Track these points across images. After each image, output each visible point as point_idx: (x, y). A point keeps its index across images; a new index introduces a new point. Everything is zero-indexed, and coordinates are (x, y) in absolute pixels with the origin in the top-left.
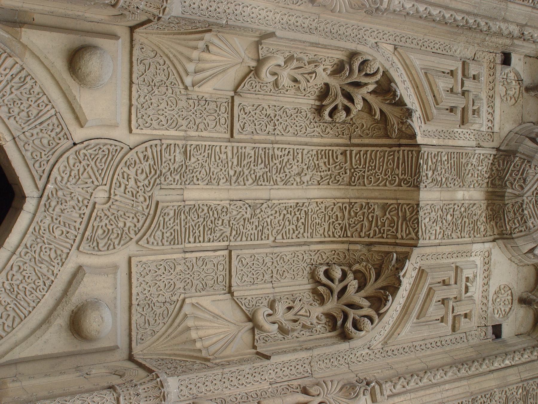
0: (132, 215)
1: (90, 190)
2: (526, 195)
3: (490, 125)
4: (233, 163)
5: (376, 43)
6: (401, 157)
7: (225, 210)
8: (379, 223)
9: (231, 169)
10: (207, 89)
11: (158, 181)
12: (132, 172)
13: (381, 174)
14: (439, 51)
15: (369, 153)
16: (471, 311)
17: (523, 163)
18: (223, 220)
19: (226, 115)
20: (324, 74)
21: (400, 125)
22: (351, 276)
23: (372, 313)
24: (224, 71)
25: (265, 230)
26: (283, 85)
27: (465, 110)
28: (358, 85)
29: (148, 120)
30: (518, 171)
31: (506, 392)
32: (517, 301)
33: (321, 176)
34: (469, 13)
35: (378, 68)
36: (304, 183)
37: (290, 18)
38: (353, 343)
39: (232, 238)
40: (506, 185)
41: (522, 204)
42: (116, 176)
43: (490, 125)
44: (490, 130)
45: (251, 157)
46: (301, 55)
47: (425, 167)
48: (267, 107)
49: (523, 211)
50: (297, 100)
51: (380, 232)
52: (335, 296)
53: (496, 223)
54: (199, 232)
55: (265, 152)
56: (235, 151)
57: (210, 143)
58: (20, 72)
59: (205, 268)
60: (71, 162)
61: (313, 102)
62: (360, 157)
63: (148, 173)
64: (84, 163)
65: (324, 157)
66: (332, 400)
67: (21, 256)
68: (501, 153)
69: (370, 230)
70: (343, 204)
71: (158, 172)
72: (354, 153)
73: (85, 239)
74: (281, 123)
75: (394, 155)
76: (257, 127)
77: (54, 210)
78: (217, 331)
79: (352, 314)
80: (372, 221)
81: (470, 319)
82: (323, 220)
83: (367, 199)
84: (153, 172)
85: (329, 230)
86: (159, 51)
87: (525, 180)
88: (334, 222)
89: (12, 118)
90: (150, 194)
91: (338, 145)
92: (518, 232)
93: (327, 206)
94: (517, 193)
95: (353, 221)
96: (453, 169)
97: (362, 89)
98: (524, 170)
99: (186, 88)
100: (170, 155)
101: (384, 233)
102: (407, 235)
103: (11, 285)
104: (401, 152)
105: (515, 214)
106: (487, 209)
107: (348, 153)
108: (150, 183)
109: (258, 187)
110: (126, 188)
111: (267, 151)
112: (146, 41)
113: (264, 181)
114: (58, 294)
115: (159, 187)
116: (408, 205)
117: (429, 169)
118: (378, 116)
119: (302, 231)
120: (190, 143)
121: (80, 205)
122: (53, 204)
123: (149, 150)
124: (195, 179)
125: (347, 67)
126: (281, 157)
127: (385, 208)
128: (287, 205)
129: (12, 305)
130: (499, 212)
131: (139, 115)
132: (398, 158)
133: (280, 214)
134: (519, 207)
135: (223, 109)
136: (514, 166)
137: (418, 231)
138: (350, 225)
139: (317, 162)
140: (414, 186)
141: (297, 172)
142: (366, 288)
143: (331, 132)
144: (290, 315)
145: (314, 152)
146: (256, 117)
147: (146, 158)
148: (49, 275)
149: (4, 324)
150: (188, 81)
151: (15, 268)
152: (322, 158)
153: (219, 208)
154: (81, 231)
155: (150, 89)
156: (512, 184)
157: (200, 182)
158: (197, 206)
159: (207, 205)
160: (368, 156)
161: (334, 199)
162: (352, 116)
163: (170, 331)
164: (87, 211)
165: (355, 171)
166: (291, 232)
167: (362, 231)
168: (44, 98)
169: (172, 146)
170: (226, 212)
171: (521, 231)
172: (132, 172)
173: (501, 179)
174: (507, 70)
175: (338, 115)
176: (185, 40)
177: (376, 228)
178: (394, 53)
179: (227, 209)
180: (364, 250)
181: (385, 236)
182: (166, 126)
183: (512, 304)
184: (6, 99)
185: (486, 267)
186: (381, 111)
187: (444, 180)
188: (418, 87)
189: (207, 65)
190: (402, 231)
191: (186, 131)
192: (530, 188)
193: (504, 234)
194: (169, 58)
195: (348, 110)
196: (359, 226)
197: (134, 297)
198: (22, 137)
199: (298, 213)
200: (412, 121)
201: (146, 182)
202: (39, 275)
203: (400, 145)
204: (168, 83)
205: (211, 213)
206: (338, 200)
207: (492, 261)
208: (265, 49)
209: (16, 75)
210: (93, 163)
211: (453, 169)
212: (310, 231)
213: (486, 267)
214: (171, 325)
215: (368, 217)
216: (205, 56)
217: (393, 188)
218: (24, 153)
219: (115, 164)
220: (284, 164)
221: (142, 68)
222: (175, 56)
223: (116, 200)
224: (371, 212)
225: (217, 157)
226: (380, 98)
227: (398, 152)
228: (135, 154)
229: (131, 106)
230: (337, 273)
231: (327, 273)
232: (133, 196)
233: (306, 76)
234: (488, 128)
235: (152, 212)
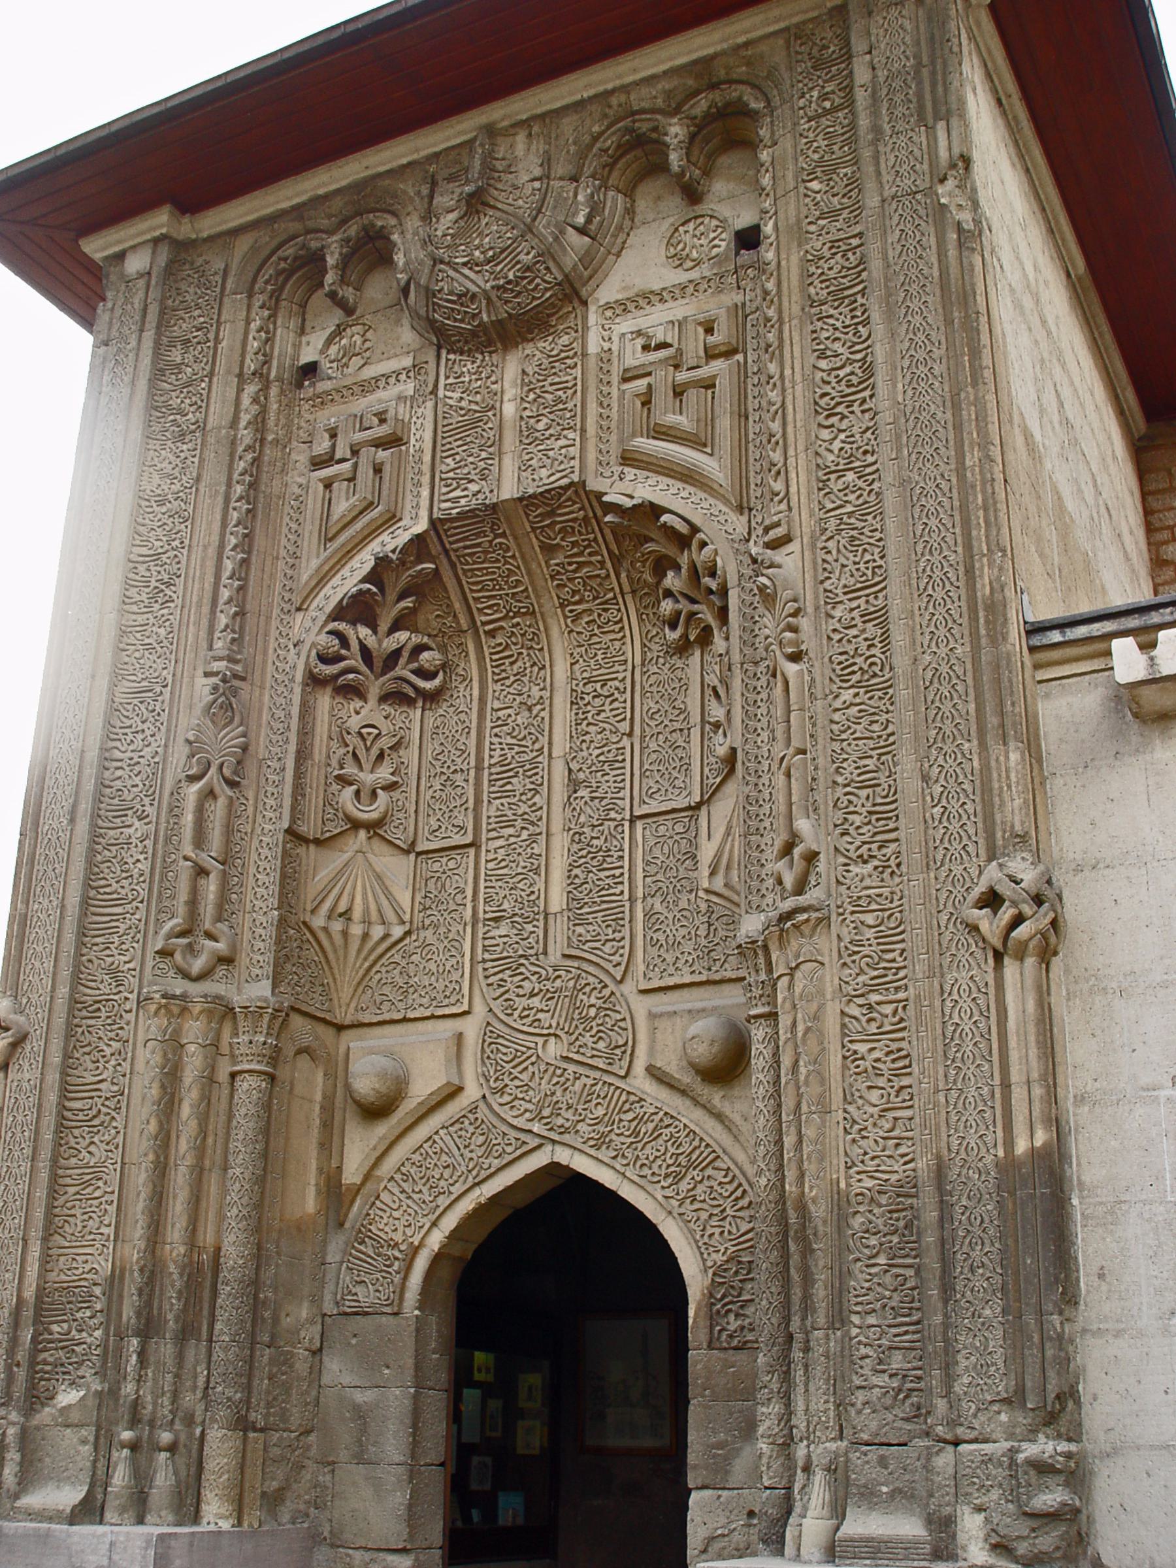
0: (581, 996)
1: (543, 1067)
2: (482, 284)
3: (403, 377)
4: (511, 836)
5: (295, 646)
6: (461, 544)
7: (577, 838)
8: (575, 550)
9: (518, 836)
11: (533, 960)
12: (520, 1003)
13: (499, 568)
15: (475, 595)
16: (700, 324)
17: (440, 306)
18: (592, 838)
19: (444, 860)
20: (363, 712)
21: (409, 565)
24: (379, 877)
25: (611, 756)
26: (392, 774)
27: (378, 442)
28: (366, 653)
29: (451, 987)
30: (453, 310)
31: (810, 223)
32: (696, 208)
33: (532, 666)
34: (227, 500)
35: (329, 633)
36: (541, 697)
37: (268, 807)
39: (619, 817)
41: (498, 288)
42: (525, 1028)
43: (403, 377)
44: (411, 374)
45: (502, 805)
46: (334, 763)
47: (463, 501)
48: (431, 790)
49: (509, 282)
51: (589, 546)
53: (549, 316)
54: (607, 877)
55: (496, 780)
56: (494, 834)
57: (482, 881)
59: (662, 858)
60: (507, 1098)
63: (521, 977)
64: (507, 1081)
65: (503, 667)
67: (628, 1165)
69: (591, 562)
70: (566, 617)
71: (522, 961)
72: (484, 619)
73: (609, 1068)
75: (463, 556)
76: (458, 804)
77: (568, 1120)
80: (576, 563)
81: (714, 321)
82: (598, 646)
84: (522, 969)
85: (613, 631)
86: (364, 983)
87: (460, 296)
88: (599, 627)
89: (451, 1188)
90: (550, 970)
92: (551, 273)
93: (575, 643)
94: (484, 302)
95: (587, 593)
96: (468, 439)
97: (369, 646)
99: (408, 933)
100: (498, 945)
101: (588, 539)
102: (574, 503)
103: (667, 1176)
104: (455, 546)
105: (520, 293)
106: (532, 340)
107: (487, 628)
108: (536, 973)
109: (546, 783)
110: (542, 1010)
111: (495, 777)
112: (353, 1005)
113: (537, 774)
114: (688, 1102)
115: (541, 957)
116: (527, 515)
117: (465, 493)
118: (408, 603)
119: (616, 683)
120: (481, 915)
121: (562, 1079)
122: (560, 1121)
123: (490, 980)
124: (532, 897)
125: (340, 681)
126: (502, 749)
127: (549, 550)
128: (573, 723)
129: (695, 1173)
130: (528, 321)
131: (446, 1002)
132: (466, 547)
133: (587, 733)
134: (506, 290)
135: (436, 866)
136: (448, 319)
137: (560, 487)
138: (595, 598)
139: (512, 679)
140: (495, 512)
141: (527, 714)
143: (462, 665)
145: (498, 687)
146: (444, 808)
148: (657, 1118)
149: (720, 1183)
150: (398, 931)
151: (646, 1171)
152: (504, 671)
153: (575, 847)
154: (597, 1074)
155: (411, 990)
157: (536, 890)
158: (570, 888)
159: (570, 871)
160: (481, 594)
162: (426, 639)
164: (572, 1068)
165: (511, 610)
166: (616, 705)
167: (598, 576)
169: (487, 943)
170: (580, 834)
171: (547, 268)
173: (474, 333)
174: (325, 365)
175: (427, 665)
176: (335, 951)
177: (586, 553)
178: (306, 609)
179: (575, 833)
181: (592, 536)
183: (703, 216)
184: (428, 1199)
185: (631, 306)
186: (401, 597)
187: (484, 455)
188: (348, 552)
189: (373, 907)
190: (572, 512)
191: (465, 924)
192: (472, 281)
193: (565, 295)
194: (371, 967)
195: (420, 649)
196: (594, 583)
197: (697, 978)
198: (474, 1173)
199: (587, 698)
200: (393, 551)
201: (534, 978)
202: (655, 1134)
203: (446, 552)
204: (403, 963)
205: (583, 860)
206: (564, 626)
207: (620, 297)
208: (329, 826)
209: (400, 1186)
210: (508, 1066)
211: (468, 439)
212: (617, 668)
213: (631, 306)
215: (575, 571)
216: (357, 914)
218: (492, 1170)
219: (508, 1031)
220: (514, 741)
221: (385, 1007)
222: (365, 959)
223: (558, 1024)
224: (563, 568)
225: (503, 864)
226: (378, 611)
227: (456, 550)
228: (498, 1001)
229: (433, 1017)
230: (667, 606)
232: (553, 998)
233: (368, 743)
234: (409, 377)
235: (576, 964)
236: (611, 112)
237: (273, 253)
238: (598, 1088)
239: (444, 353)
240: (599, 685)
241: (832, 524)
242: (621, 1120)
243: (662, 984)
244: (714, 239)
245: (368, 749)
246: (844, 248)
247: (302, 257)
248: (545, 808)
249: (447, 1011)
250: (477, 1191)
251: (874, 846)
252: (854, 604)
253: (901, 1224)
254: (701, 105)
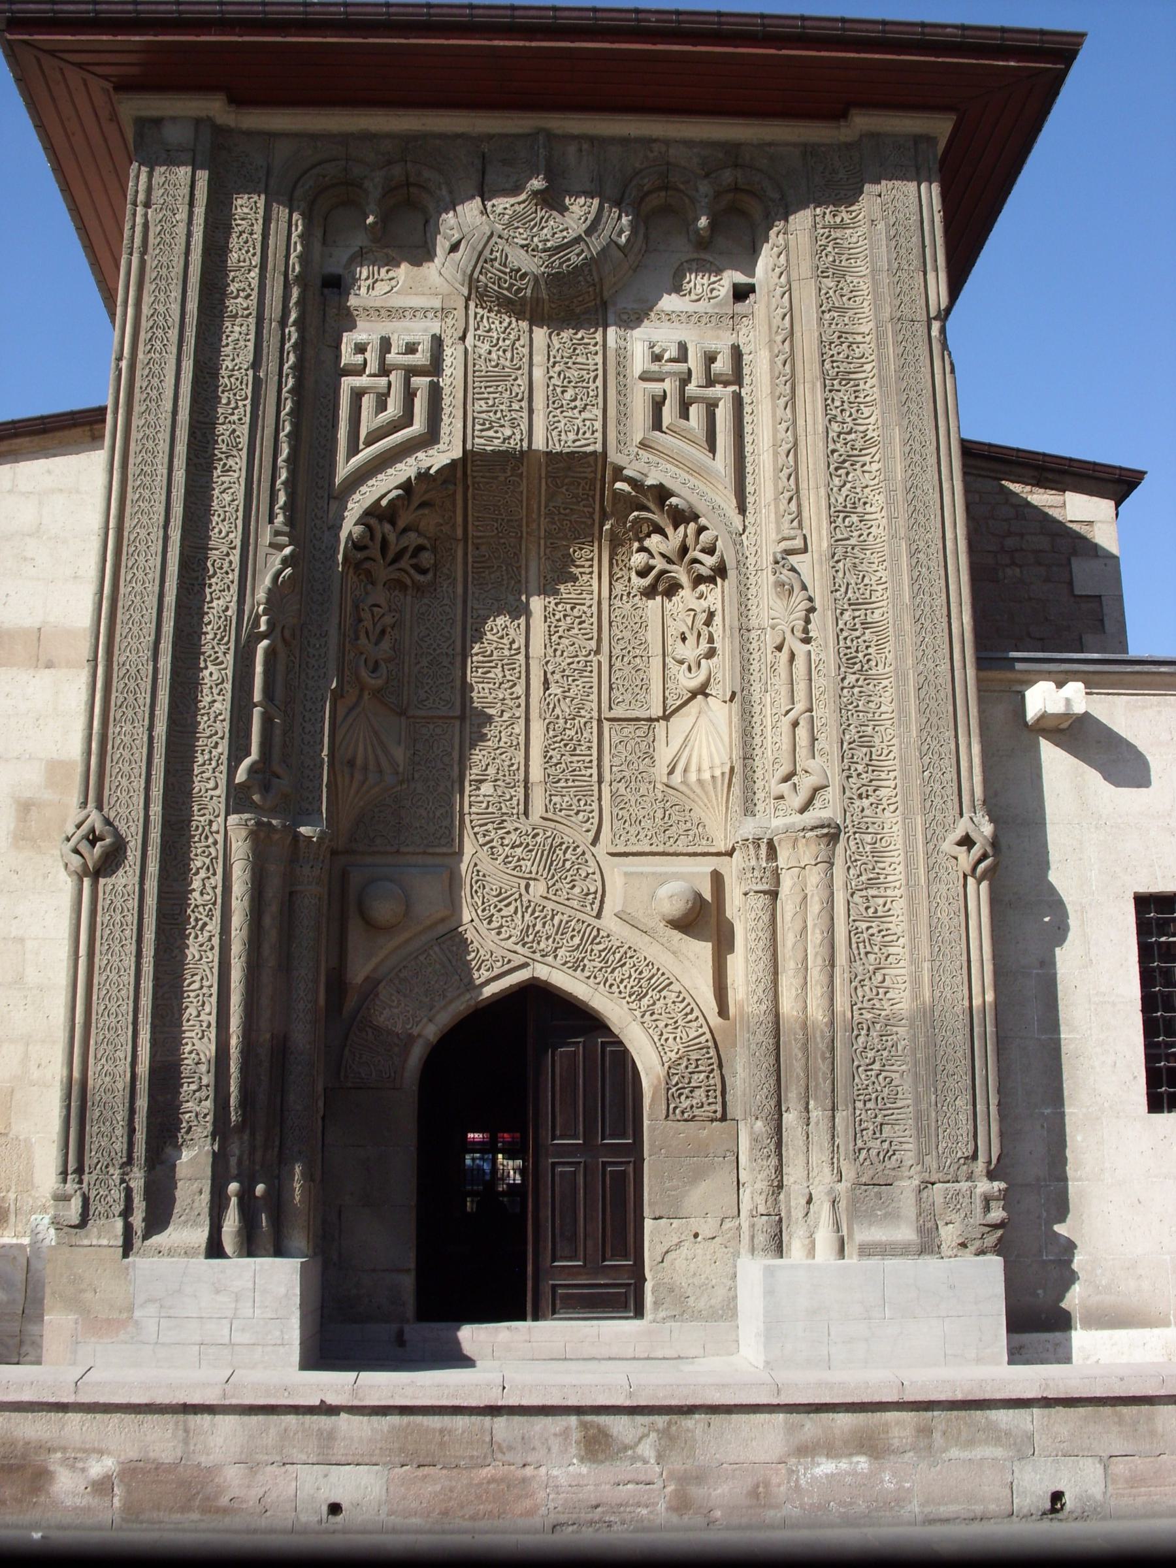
3: (430, 315)
5: (329, 529)
10: (399, 754)
14: (330, 417)
19: (431, 726)
23: (692, 526)
30: (500, 278)
38: (730, 564)
43: (430, 315)
44: (438, 314)
50: (408, 624)
51: (587, 499)
61: (409, 598)
66: (792, 617)
68: (473, 296)
70: (546, 547)
74: (439, 645)
78: (704, 744)
83: (539, 515)
91: (466, 554)
136: (494, 283)
143: (448, 565)
161: (540, 559)
168: (422, 958)
171: (590, 270)
191: (453, 782)
195: (420, 548)
206: (542, 554)
207: (635, 306)
216: (359, 761)
227: (474, 477)
231: (642, 574)
236: (651, 155)
237: (314, 166)
238: (573, 923)
239: (472, 305)
240: (569, 606)
241: (840, 551)
242: (592, 950)
243: (627, 850)
244: (714, 283)
245: (374, 625)
246: (851, 340)
248: (523, 697)
249: (438, 850)
251: (871, 789)
252: (857, 614)
253: (890, 1043)
254: (727, 176)
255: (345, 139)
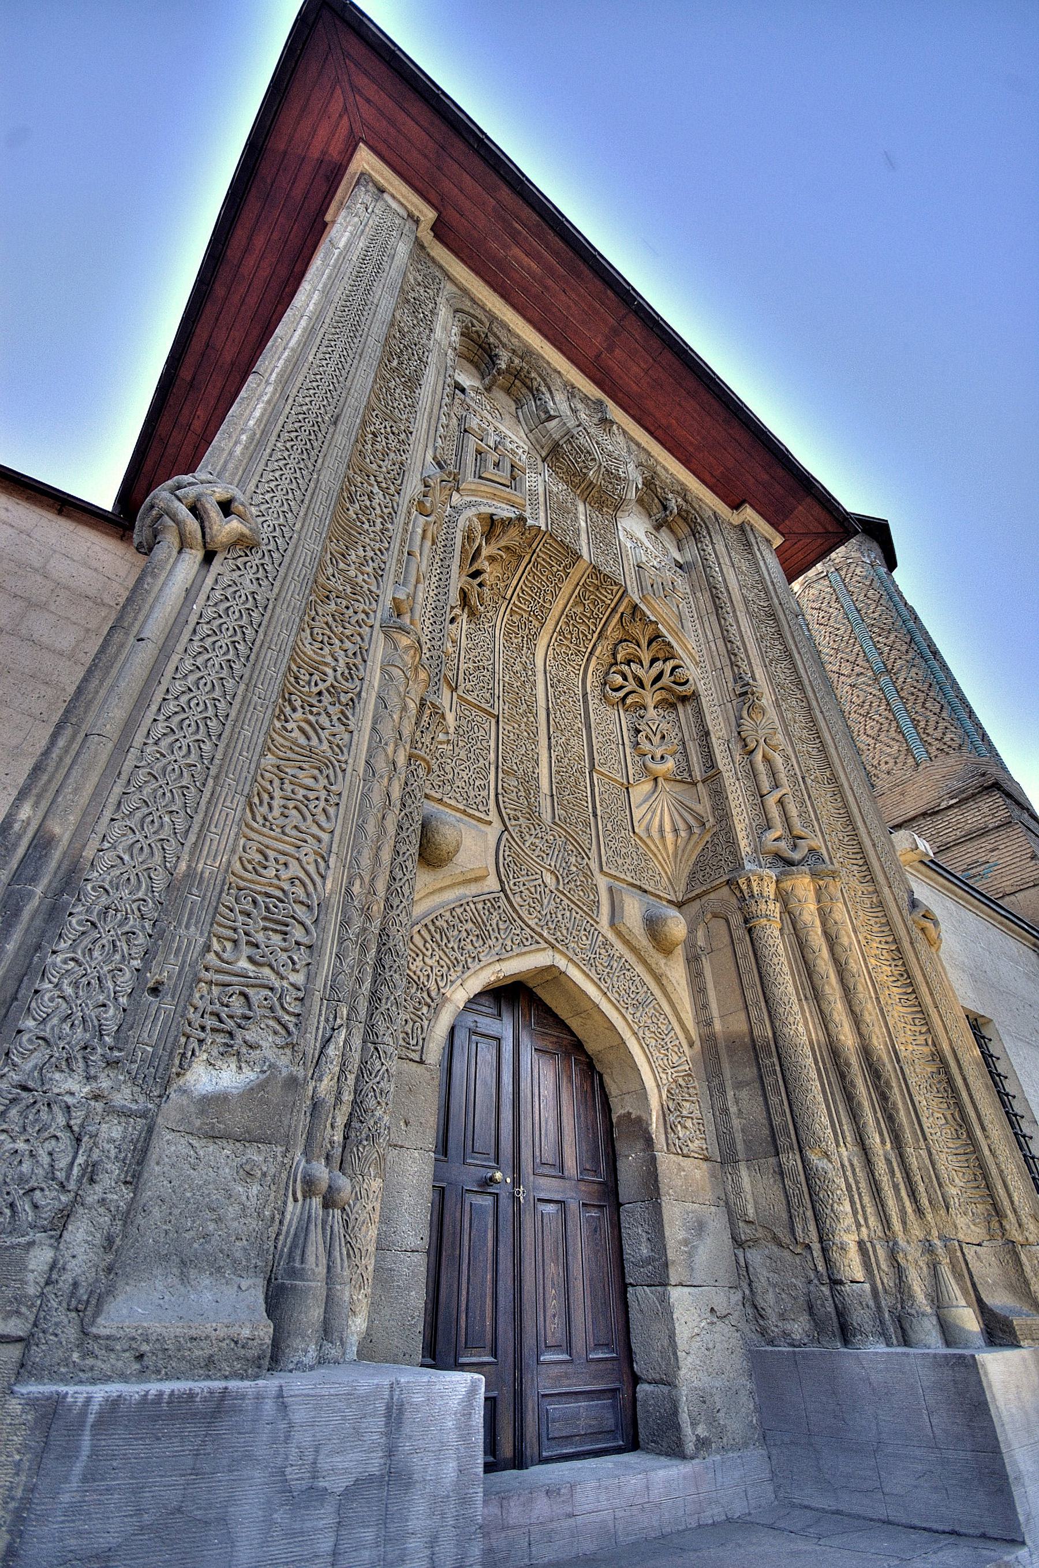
12: (530, 840)
22: (625, 668)
23: (671, 664)
40: (585, 474)
52: (640, 690)
58: (429, 931)
62: (524, 599)
64: (522, 888)
79: (666, 680)
83: (562, 613)
87: (588, 452)
98: (579, 448)
104: (541, 554)
123: (508, 811)
132: (543, 560)
142: (642, 658)
143: (491, 614)
144: (656, 740)
147: (517, 819)
156: (586, 467)
163: (660, 858)
164: (566, 901)
168: (459, 910)
172: (530, 840)
180: (605, 643)
182: (486, 782)
210: (521, 879)
214: (655, 855)
217: (566, 583)
227: (538, 556)
247: (479, 336)
250: (497, 967)
255: (493, 318)
